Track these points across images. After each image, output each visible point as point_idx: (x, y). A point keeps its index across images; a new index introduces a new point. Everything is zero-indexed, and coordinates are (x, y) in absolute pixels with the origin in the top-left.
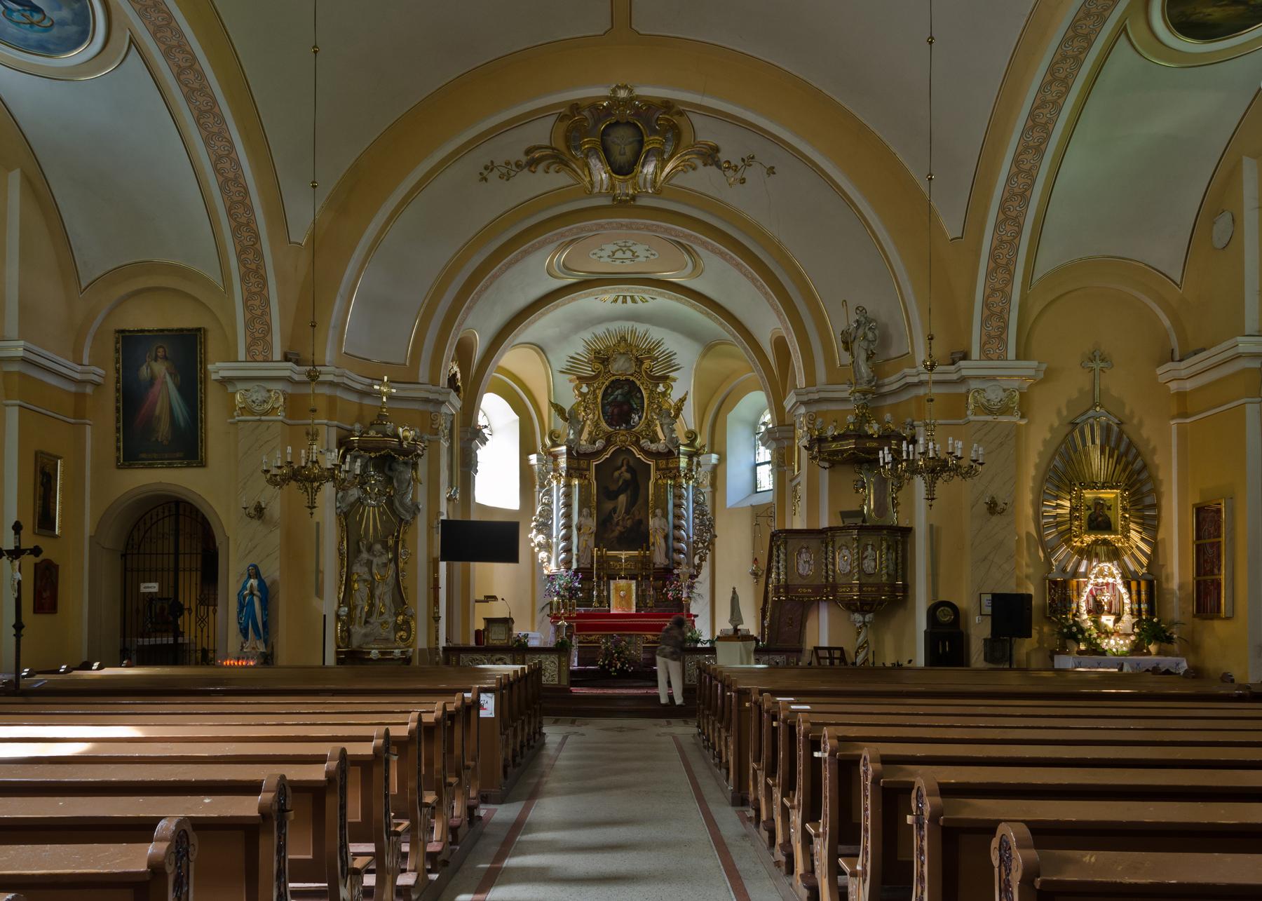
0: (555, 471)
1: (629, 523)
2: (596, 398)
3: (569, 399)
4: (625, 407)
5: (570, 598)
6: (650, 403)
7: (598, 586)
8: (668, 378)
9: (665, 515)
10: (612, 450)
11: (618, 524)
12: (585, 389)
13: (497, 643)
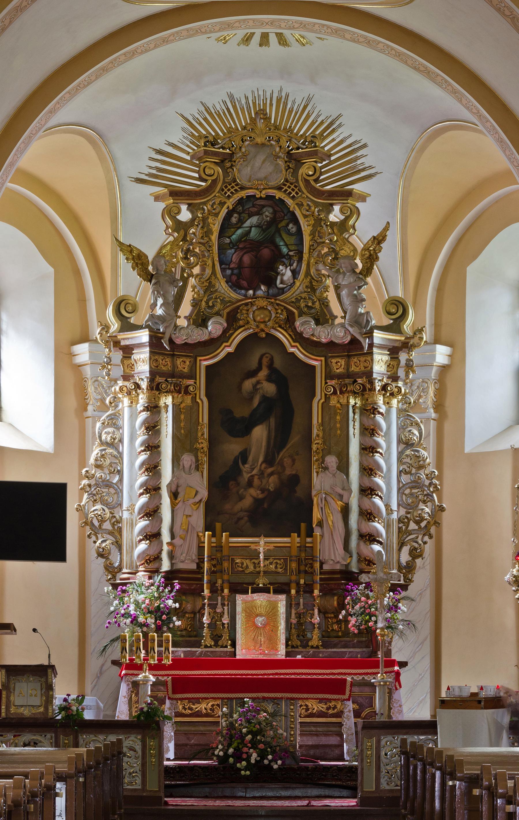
0: (126, 378)
1: (272, 483)
2: (208, 233)
3: (153, 238)
4: (266, 252)
5: (159, 629)
6: (316, 244)
7: (213, 607)
8: (349, 194)
9: (344, 467)
10: (239, 336)
11: (250, 484)
12: (185, 215)
13: (26, 712)
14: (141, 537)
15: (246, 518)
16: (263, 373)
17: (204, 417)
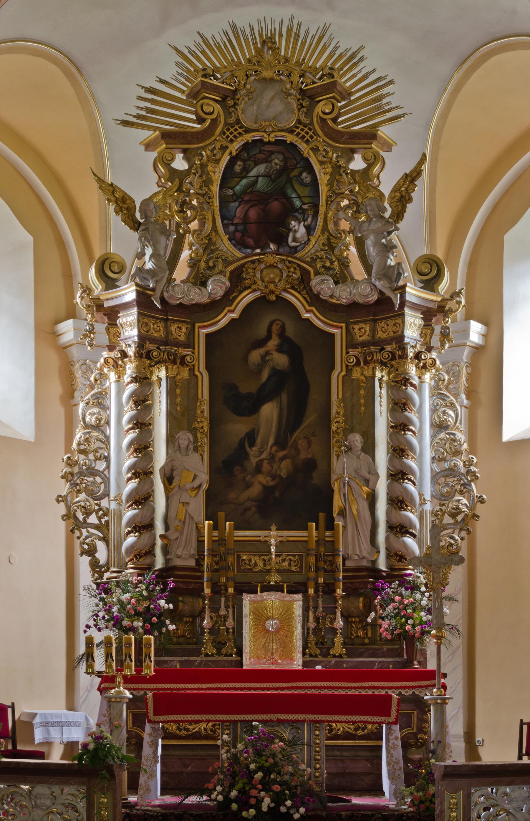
1: (284, 468)
11: (258, 469)
15: (254, 509)
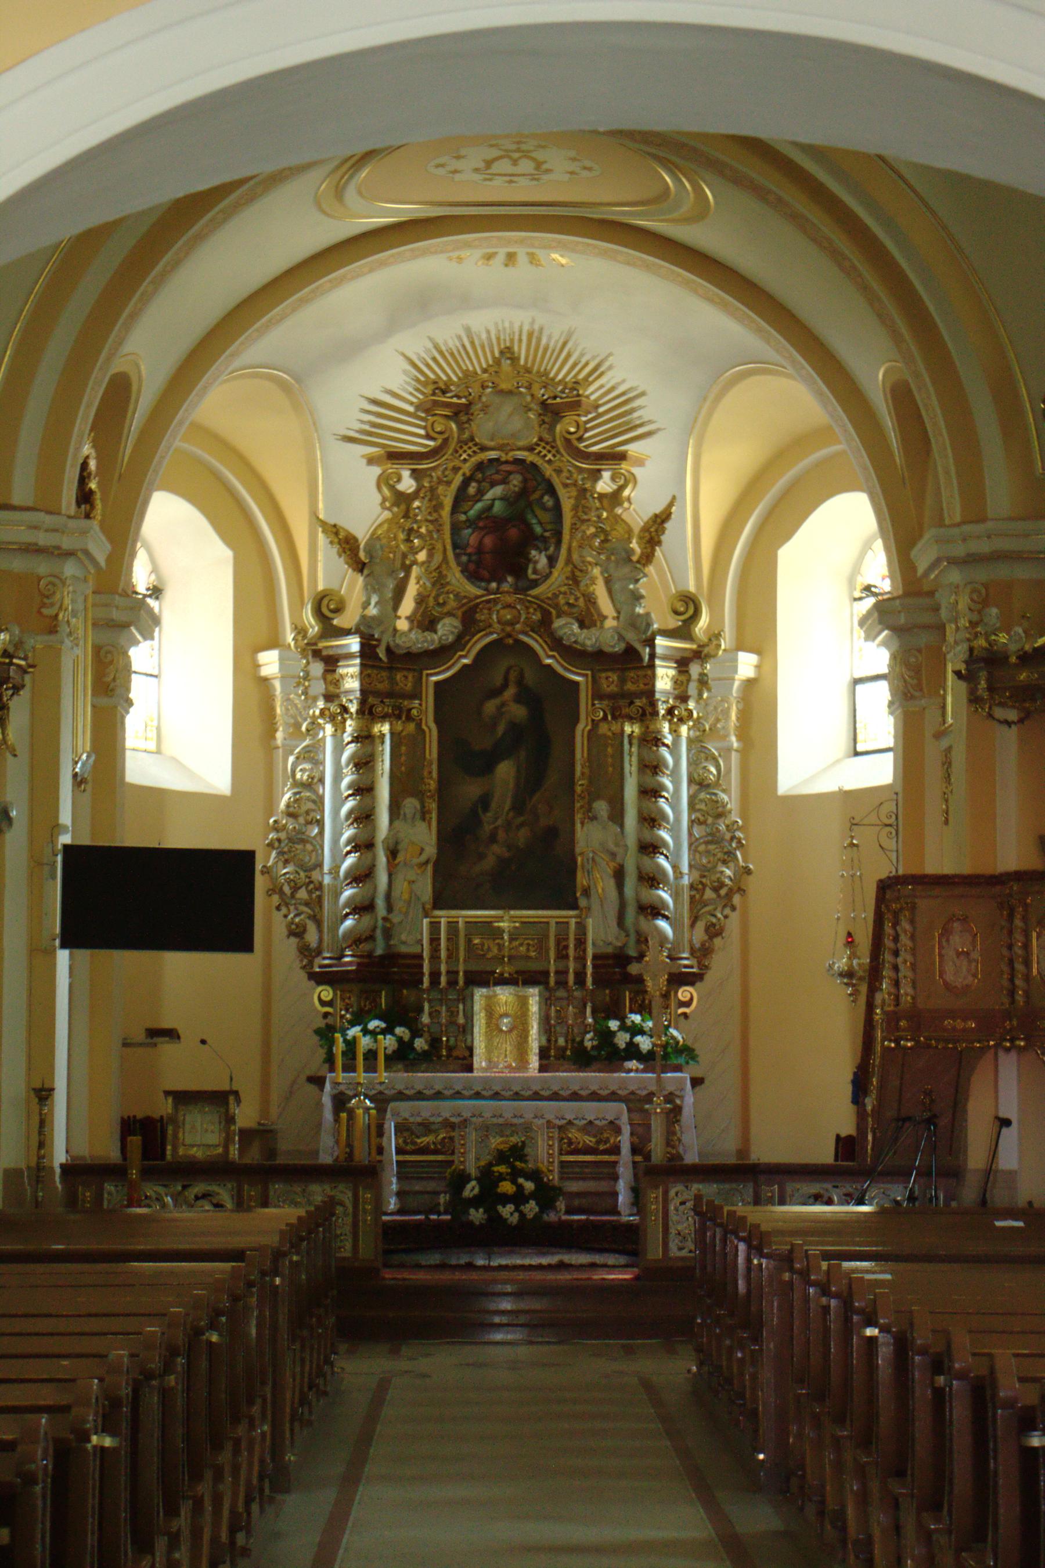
1: (523, 836)
11: (493, 838)
12: (407, 484)
14: (348, 910)
16: (510, 692)
17: (432, 751)
